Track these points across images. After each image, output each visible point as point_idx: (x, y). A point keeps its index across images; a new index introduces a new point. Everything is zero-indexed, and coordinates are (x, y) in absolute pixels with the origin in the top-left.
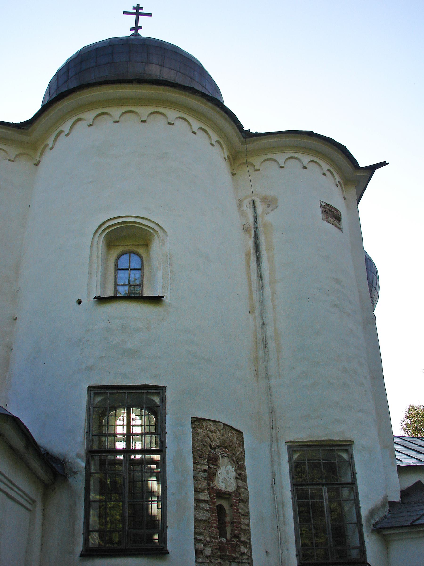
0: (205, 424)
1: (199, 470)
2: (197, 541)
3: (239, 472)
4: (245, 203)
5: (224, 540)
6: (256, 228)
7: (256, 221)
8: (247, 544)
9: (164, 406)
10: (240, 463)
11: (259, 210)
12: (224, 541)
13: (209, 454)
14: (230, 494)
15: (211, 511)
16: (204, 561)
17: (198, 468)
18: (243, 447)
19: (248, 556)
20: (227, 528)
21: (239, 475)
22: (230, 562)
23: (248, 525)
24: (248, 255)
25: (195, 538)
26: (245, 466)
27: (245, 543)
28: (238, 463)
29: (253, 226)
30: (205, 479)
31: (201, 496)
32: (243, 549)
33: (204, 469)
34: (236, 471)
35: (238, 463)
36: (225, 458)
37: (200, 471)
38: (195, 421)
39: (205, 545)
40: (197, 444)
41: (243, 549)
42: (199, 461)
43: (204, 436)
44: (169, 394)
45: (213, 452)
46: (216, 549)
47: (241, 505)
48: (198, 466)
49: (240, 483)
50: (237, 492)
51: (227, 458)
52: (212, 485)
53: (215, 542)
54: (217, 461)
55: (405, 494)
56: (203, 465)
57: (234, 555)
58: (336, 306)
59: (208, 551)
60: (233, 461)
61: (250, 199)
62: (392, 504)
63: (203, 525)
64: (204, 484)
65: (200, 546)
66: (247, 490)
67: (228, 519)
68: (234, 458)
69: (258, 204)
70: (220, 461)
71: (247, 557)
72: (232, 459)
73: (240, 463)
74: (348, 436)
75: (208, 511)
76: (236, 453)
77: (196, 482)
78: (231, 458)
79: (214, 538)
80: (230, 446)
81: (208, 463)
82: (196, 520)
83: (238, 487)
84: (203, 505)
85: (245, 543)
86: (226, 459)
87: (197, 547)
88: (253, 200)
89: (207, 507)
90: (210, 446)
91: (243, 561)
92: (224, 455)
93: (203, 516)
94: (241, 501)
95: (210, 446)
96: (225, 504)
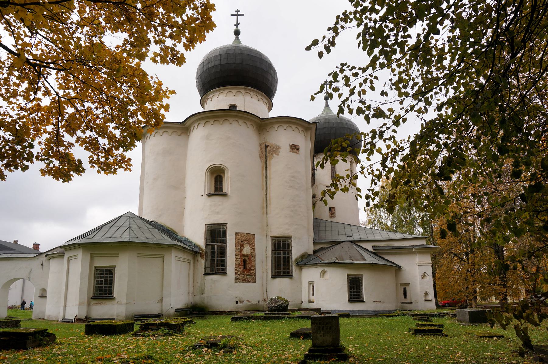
2: (236, 270)
8: (254, 270)
14: (248, 255)
15: (241, 261)
24: (263, 168)
27: (253, 270)
31: (237, 257)
32: (252, 272)
41: (252, 272)
44: (228, 226)
47: (252, 258)
49: (252, 251)
55: (315, 252)
58: (291, 187)
59: (239, 273)
62: (309, 255)
63: (238, 265)
64: (239, 253)
65: (236, 271)
67: (247, 263)
70: (245, 245)
74: (290, 234)
82: (235, 264)
83: (251, 253)
84: (238, 259)
85: (253, 270)
86: (247, 244)
89: (239, 260)
93: (238, 263)
94: (253, 257)
96: (246, 258)
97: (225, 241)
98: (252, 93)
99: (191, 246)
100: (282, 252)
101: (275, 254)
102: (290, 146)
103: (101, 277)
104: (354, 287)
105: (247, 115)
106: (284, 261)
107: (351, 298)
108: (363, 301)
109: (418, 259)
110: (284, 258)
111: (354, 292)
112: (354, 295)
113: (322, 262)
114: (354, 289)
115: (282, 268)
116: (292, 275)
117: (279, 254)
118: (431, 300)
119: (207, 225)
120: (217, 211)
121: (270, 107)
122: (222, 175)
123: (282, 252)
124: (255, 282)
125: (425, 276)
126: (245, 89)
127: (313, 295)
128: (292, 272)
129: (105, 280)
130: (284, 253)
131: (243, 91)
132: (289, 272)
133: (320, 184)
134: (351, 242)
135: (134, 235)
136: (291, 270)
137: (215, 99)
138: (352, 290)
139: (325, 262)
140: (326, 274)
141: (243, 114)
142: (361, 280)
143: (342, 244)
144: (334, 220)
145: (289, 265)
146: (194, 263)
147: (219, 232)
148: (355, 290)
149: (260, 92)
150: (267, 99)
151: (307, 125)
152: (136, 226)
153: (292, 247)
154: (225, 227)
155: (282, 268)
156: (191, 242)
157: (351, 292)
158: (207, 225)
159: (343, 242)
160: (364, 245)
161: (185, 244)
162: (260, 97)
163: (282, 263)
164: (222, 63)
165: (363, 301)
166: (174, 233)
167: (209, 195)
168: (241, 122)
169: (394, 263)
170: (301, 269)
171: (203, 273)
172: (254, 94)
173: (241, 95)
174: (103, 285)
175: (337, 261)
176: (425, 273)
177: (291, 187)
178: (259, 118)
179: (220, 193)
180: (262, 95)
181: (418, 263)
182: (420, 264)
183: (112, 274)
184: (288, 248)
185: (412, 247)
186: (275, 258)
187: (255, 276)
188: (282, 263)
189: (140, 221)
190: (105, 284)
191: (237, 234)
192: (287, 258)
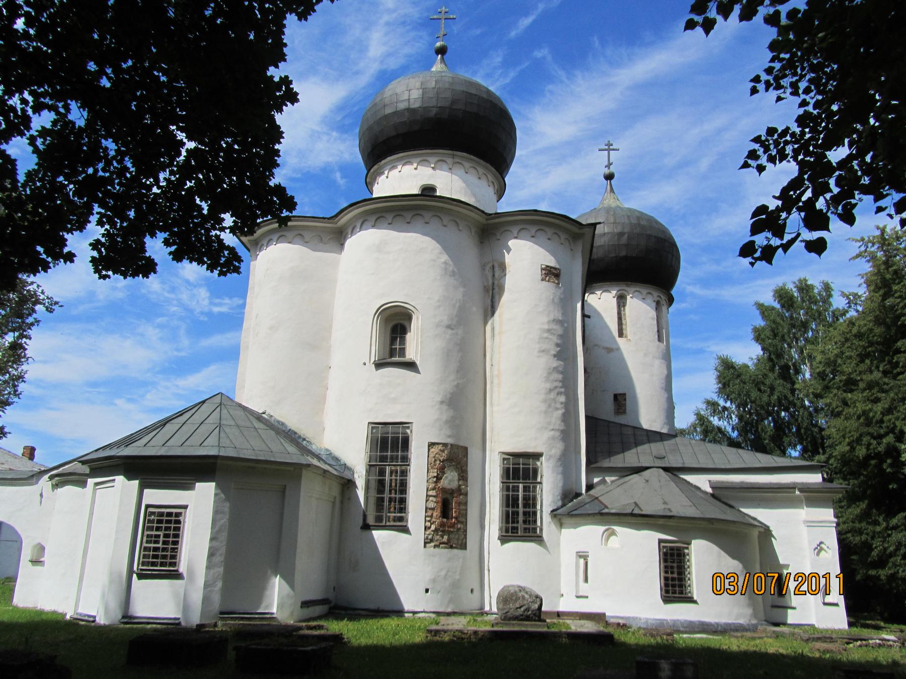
0: (437, 446)
3: (462, 475)
4: (488, 267)
5: (445, 520)
6: (493, 289)
7: (493, 284)
11: (497, 275)
23: (466, 510)
28: (461, 468)
29: (491, 287)
31: (431, 493)
34: (459, 475)
35: (461, 468)
39: (431, 524)
57: (452, 530)
59: (433, 527)
61: (490, 265)
65: (428, 524)
68: (458, 466)
69: (496, 269)
75: (435, 502)
83: (460, 486)
84: (431, 498)
85: (462, 523)
88: (493, 266)
90: (440, 460)
95: (440, 460)
97: (406, 459)
98: (467, 165)
99: (337, 467)
100: (521, 486)
101: (508, 489)
102: (542, 269)
103: (158, 529)
104: (672, 567)
105: (459, 206)
106: (525, 506)
107: (667, 592)
108: (691, 600)
109: (804, 513)
110: (526, 499)
111: (673, 579)
112: (673, 586)
113: (606, 511)
114: (672, 573)
115: (521, 518)
116: (541, 537)
117: (516, 489)
118: (836, 605)
119: (374, 425)
120: (393, 396)
121: (500, 192)
122: (406, 323)
123: (521, 486)
124: (465, 548)
125: (821, 549)
126: (453, 156)
127: (586, 580)
128: (541, 530)
129: (166, 536)
130: (526, 489)
131: (450, 160)
132: (535, 529)
133: (596, 345)
134: (666, 469)
135: (228, 442)
136: (539, 523)
137: (394, 173)
138: (670, 575)
139: (613, 511)
140: (613, 538)
141: (452, 204)
142: (688, 554)
143: (646, 473)
144: (621, 419)
145: (535, 513)
146: (342, 502)
147: (395, 440)
148: (675, 575)
149: (482, 161)
150: (495, 176)
151: (575, 229)
152: (232, 423)
153: (541, 477)
154: (408, 431)
155: (521, 518)
156: (337, 459)
157: (666, 579)
158: (374, 425)
159: (647, 468)
160: (691, 478)
161: (326, 463)
162: (481, 170)
163: (521, 509)
164: (412, 106)
165: (691, 600)
166: (304, 439)
167: (379, 365)
168: (446, 220)
169: (755, 519)
170: (561, 525)
171: (361, 523)
172: (470, 165)
173: (445, 166)
174: (160, 545)
175: (636, 511)
176: (821, 543)
177: (543, 351)
178: (483, 212)
179: (402, 359)
180: (486, 168)
181: (806, 522)
182: (810, 524)
183: (179, 522)
184: (535, 476)
185: (791, 487)
186: (508, 496)
187: (466, 536)
188: (521, 509)
189: (240, 413)
190: (164, 543)
191: (431, 445)
192: (530, 502)
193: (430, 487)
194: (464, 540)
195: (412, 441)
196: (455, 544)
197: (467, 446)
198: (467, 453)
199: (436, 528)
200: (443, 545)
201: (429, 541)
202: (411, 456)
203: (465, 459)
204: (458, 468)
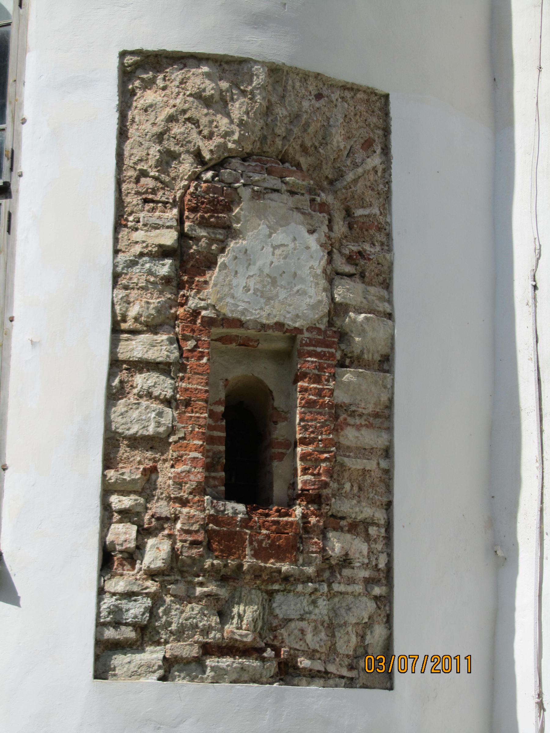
0: (177, 75)
1: (137, 249)
9: (24, 21)
10: (359, 212)
12: (236, 513)
13: (188, 187)
16: (136, 589)
17: (137, 243)
18: (386, 151)
19: (376, 568)
20: (275, 463)
21: (350, 259)
22: (271, 594)
25: (106, 507)
26: (389, 224)
28: (348, 213)
30: (167, 280)
33: (160, 246)
35: (348, 213)
36: (275, 196)
37: (142, 255)
38: (137, 66)
40: (139, 153)
42: (141, 215)
43: (171, 119)
45: (209, 175)
46: (195, 544)
48: (139, 235)
50: (331, 324)
51: (285, 197)
52: (192, 303)
53: (190, 517)
54: (228, 209)
56: (156, 227)
57: (285, 567)
60: (323, 207)
66: (390, 316)
71: (366, 574)
72: (313, 201)
73: (359, 212)
75: (168, 402)
76: (341, 175)
77: (120, 293)
78: (307, 197)
79: (184, 503)
80: (304, 149)
81: (181, 221)
87: (110, 538)
91: (336, 587)
92: (266, 185)
95: (198, 155)
193: (133, 311)
194: (379, 631)
195: (25, 50)
196: (312, 655)
197: (382, 87)
198: (387, 131)
199: (174, 554)
200: (226, 662)
201: (128, 633)
202: (17, 135)
203: (375, 161)
204: (323, 207)
